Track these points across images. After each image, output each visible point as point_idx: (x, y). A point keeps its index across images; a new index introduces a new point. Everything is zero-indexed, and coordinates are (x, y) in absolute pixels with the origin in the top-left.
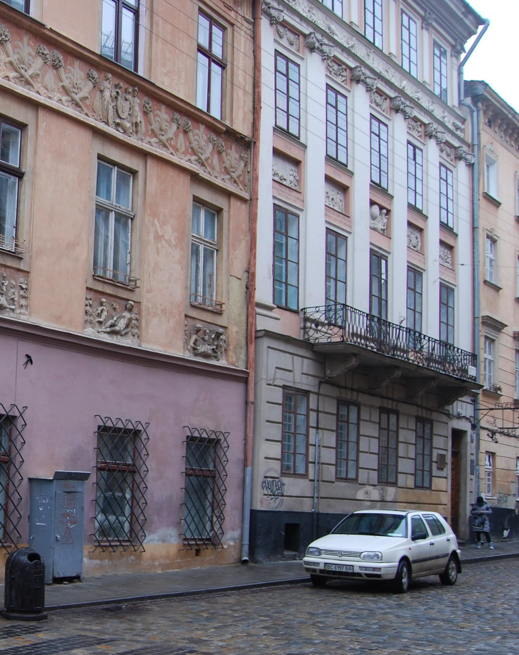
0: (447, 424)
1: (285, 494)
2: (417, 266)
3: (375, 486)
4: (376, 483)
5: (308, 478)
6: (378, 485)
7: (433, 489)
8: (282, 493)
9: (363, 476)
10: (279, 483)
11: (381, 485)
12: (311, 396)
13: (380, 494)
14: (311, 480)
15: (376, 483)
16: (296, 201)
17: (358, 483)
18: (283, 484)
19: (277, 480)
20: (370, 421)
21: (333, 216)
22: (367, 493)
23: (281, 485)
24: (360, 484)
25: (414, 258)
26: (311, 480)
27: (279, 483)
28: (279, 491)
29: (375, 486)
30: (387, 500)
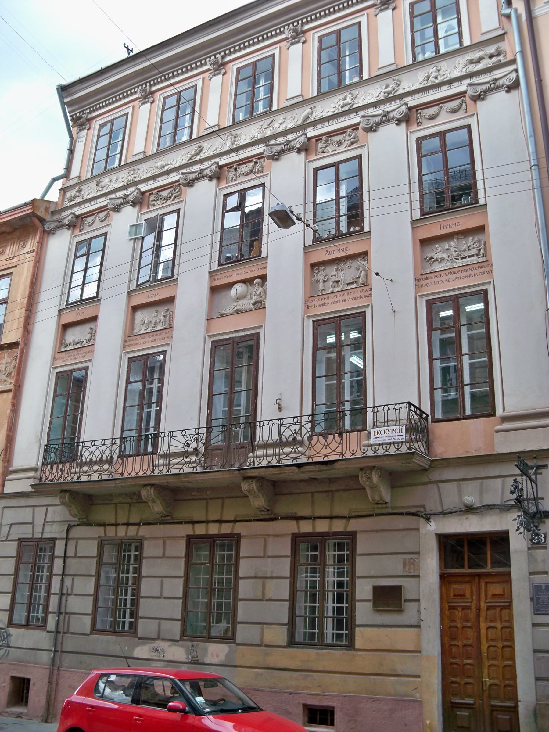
0: (418, 529)
1: (11, 646)
2: (339, 311)
3: (177, 641)
4: (178, 638)
5: (45, 630)
6: (181, 640)
7: (356, 647)
8: (8, 644)
9: (145, 627)
10: (5, 634)
11: (192, 641)
12: (57, 542)
13: (187, 653)
14: (48, 632)
15: (178, 638)
16: (85, 356)
17: (136, 636)
18: (9, 635)
19: (3, 631)
20: (163, 557)
21: (142, 341)
22: (157, 650)
23: (7, 636)
24: (139, 639)
25: (336, 303)
26: (48, 632)
27: (5, 634)
28: (4, 642)
29: (177, 641)
30: (207, 661)
